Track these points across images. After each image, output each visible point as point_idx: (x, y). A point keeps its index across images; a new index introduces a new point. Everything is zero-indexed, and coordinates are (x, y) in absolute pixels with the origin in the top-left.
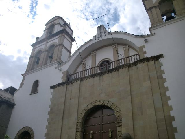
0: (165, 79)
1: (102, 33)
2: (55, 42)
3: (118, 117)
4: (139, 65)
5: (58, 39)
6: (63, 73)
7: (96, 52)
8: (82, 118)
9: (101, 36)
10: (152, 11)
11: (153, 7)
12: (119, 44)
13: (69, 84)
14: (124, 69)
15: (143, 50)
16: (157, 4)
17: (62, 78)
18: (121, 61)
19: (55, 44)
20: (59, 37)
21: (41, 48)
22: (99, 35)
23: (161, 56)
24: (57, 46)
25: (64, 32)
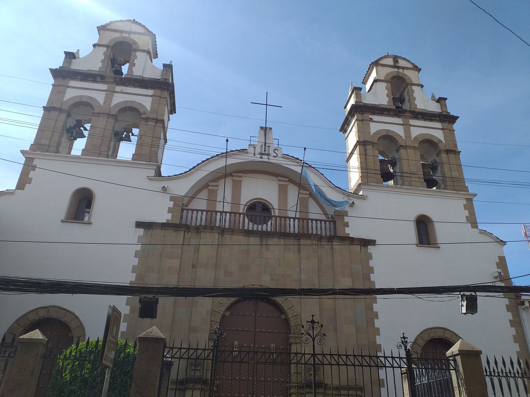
1: (268, 146)
2: (144, 106)
3: (295, 327)
4: (337, 246)
5: (150, 99)
6: (172, 199)
7: (241, 177)
8: (222, 313)
9: (267, 153)
10: (366, 150)
11: (370, 142)
12: (291, 181)
13: (189, 232)
14: (309, 242)
17: (170, 210)
19: (141, 111)
20: (152, 96)
21: (91, 98)
22: (263, 150)
23: (372, 242)
24: (147, 119)
25: (168, 89)
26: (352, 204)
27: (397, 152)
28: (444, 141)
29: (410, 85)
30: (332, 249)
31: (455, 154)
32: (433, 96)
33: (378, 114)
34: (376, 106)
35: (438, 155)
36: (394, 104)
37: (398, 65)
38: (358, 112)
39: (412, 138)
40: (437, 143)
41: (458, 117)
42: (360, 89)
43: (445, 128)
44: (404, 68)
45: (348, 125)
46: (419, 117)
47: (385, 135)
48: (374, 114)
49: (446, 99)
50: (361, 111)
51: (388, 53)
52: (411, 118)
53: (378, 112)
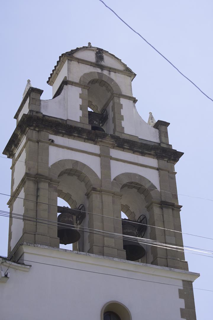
10: (38, 189)
26: (6, 278)
27: (88, 198)
29: (118, 96)
31: (173, 210)
32: (151, 118)
34: (61, 122)
35: (149, 208)
36: (90, 122)
37: (103, 63)
38: (32, 128)
39: (113, 177)
41: (183, 153)
42: (40, 92)
44: (110, 70)
45: (17, 146)
46: (126, 147)
47: (71, 170)
48: (57, 133)
49: (167, 124)
50: (37, 126)
51: (89, 44)
52: (113, 148)
53: (64, 132)
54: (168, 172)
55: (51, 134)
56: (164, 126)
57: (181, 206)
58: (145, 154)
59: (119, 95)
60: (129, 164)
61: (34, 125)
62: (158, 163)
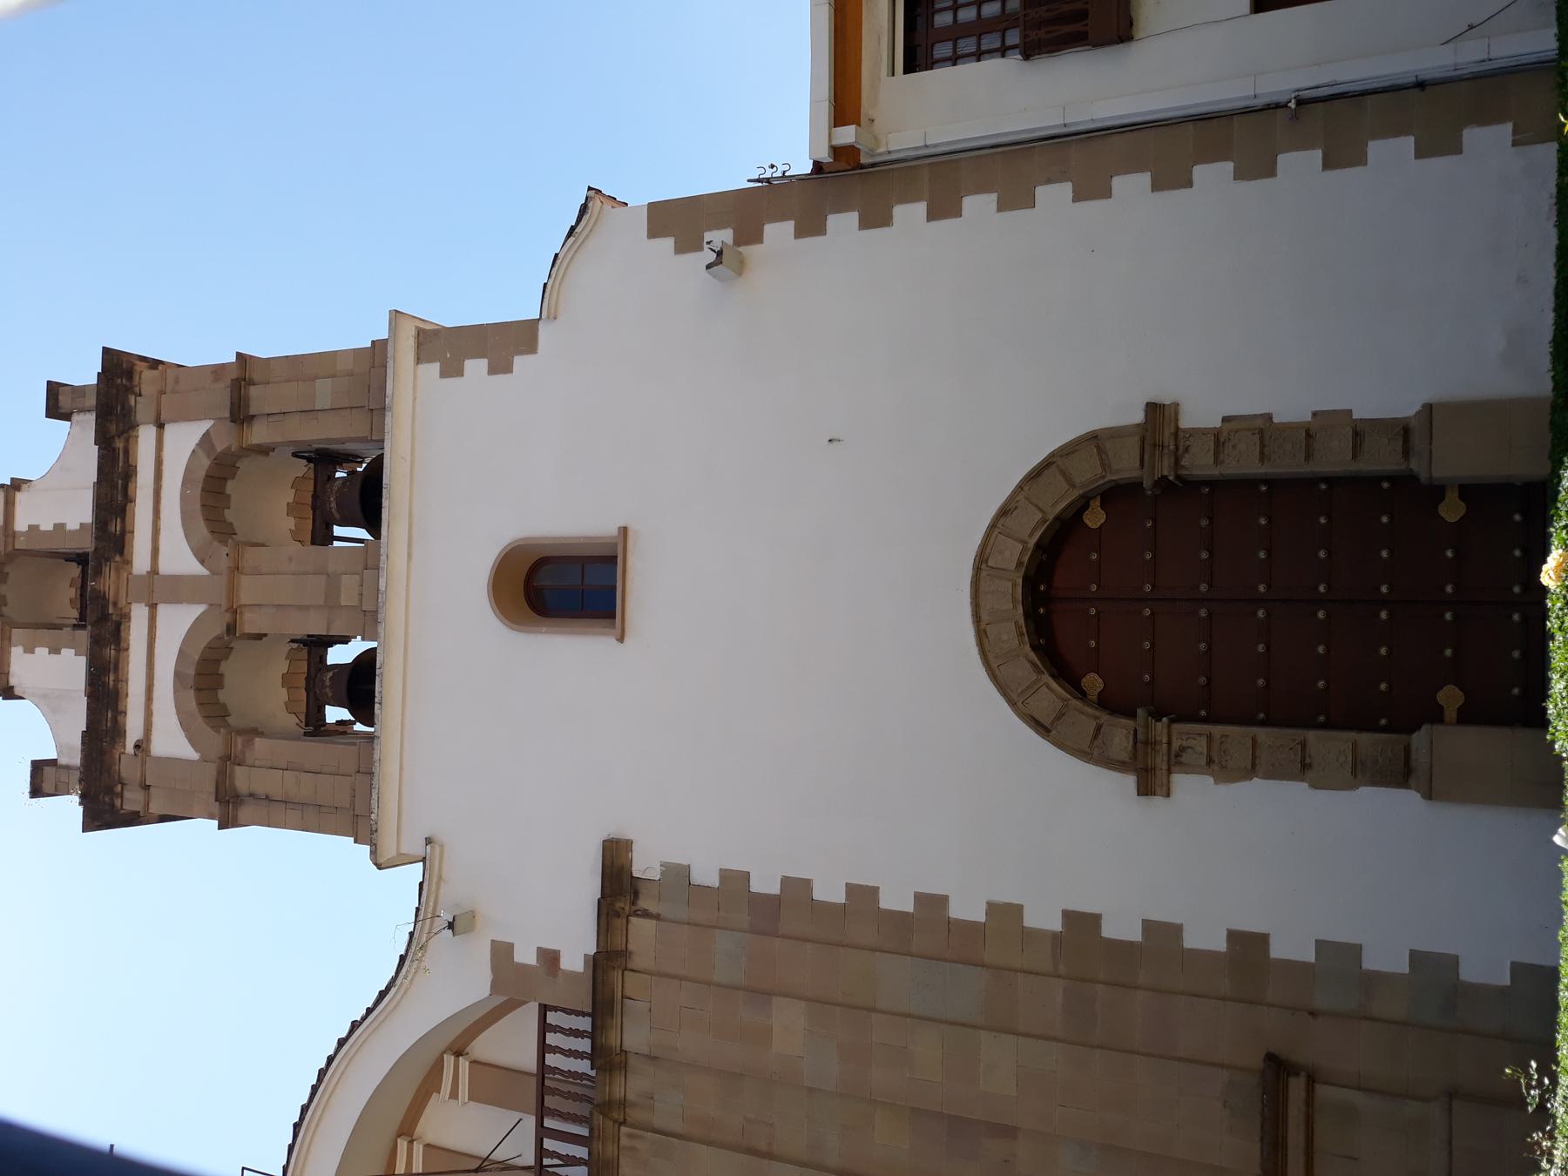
0: (786, 882)
10: (251, 795)
15: (524, 967)
16: (216, 741)
18: (546, 1161)
26: (457, 925)
28: (204, 426)
29: (10, 540)
30: (652, 1058)
31: (252, 383)
33: (119, 713)
35: (264, 450)
38: (118, 802)
39: (199, 569)
40: (213, 458)
42: (38, 767)
43: (152, 417)
46: (118, 529)
47: (198, 690)
48: (118, 732)
49: (54, 389)
50: (110, 791)
52: (129, 562)
53: (109, 714)
54: (162, 392)
55: (124, 747)
56: (60, 398)
57: (239, 355)
58: (130, 466)
59: (6, 536)
60: (162, 516)
61: (107, 799)
62: (144, 423)
